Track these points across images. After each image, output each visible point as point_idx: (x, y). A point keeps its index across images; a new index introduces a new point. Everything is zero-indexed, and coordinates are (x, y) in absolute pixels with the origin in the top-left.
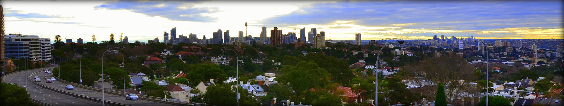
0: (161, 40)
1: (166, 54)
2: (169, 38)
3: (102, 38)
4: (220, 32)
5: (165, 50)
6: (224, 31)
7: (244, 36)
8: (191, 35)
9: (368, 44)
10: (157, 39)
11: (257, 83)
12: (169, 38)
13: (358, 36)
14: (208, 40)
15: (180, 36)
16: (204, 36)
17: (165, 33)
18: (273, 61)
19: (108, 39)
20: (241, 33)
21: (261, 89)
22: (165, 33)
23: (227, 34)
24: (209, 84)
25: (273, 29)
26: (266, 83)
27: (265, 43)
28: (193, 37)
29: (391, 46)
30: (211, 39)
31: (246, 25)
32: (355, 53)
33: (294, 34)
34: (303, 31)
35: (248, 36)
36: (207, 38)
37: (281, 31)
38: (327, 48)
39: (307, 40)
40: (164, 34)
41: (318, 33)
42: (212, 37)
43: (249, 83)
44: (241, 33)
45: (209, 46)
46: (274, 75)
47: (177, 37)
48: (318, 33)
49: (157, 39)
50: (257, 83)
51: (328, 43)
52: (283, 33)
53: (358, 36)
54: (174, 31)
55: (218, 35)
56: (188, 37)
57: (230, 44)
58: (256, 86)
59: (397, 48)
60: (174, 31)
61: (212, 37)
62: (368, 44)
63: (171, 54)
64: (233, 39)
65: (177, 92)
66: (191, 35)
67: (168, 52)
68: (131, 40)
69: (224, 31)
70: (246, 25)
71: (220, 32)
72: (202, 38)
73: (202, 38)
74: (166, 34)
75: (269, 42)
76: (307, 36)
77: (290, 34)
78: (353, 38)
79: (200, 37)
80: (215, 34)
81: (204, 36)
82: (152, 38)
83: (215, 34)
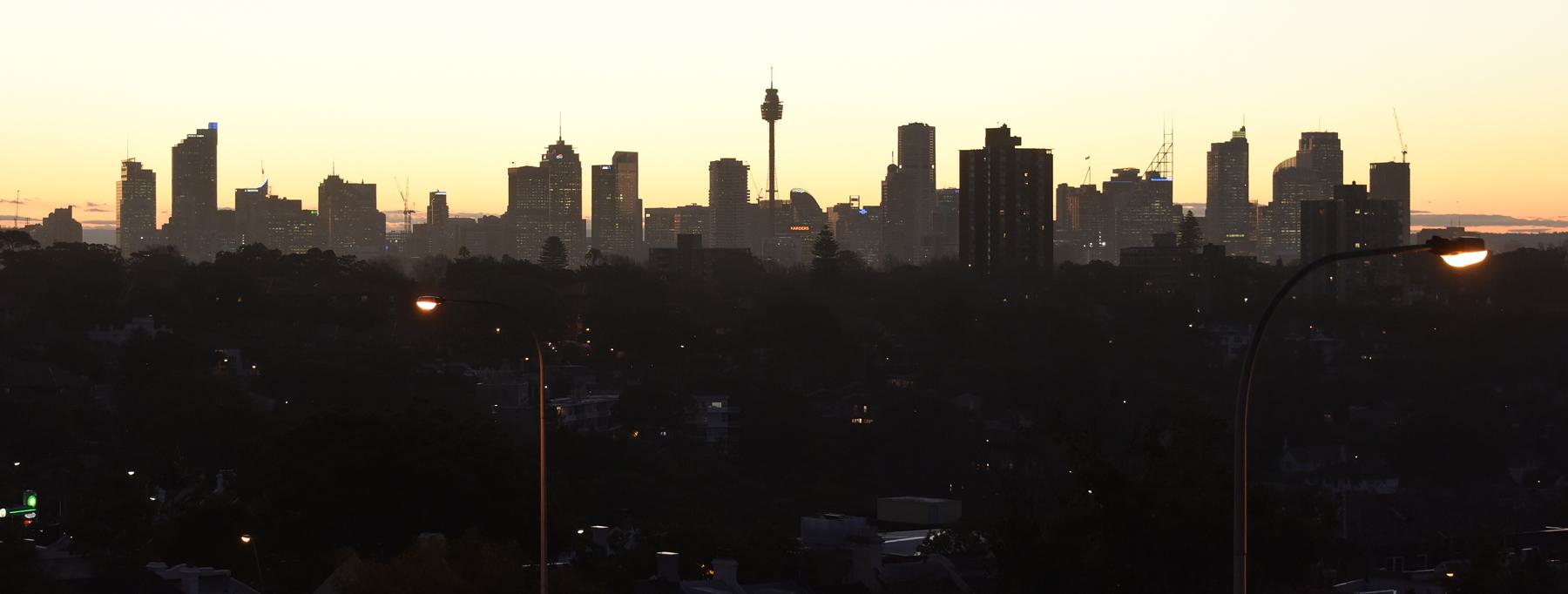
4: (562, 159)
6: (594, 154)
7: (757, 190)
8: (332, 188)
15: (241, 194)
16: (438, 201)
20: (728, 175)
25: (979, 143)
30: (488, 220)
31: (772, 109)
34: (1229, 160)
35: (783, 195)
36: (457, 206)
37: (1042, 161)
40: (117, 175)
41: (1356, 172)
44: (728, 175)
47: (226, 199)
48: (1356, 172)
52: (1066, 173)
54: (197, 156)
56: (311, 202)
66: (332, 188)
69: (594, 154)
70: (772, 109)
71: (562, 159)
74: (137, 180)
77: (1125, 178)
80: (520, 178)
81: (438, 201)
83: (520, 178)
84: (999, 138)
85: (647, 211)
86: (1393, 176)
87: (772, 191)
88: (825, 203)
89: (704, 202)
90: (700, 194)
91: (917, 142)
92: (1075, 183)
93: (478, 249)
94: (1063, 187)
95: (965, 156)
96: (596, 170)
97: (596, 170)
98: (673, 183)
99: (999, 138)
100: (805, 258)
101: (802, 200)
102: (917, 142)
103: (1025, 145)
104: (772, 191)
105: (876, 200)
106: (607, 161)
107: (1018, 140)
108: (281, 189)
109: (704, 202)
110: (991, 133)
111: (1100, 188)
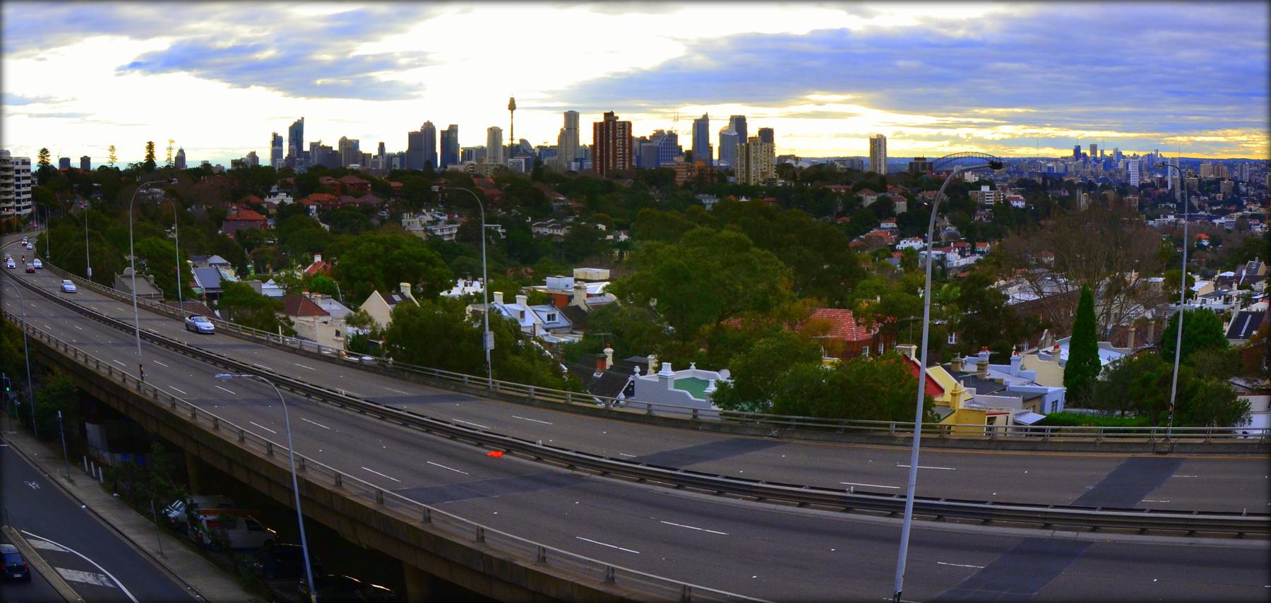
0: (265, 159)
1: (276, 201)
2: (285, 153)
3: (129, 156)
4: (429, 129)
5: (274, 189)
6: (441, 126)
7: (506, 142)
8: (344, 142)
9: (906, 169)
10: (253, 156)
11: (548, 299)
12: (285, 153)
13: (878, 144)
14: (391, 157)
15: (313, 145)
16: (382, 146)
17: (275, 135)
18: (602, 227)
19: (141, 158)
20: (495, 134)
21: (561, 320)
22: (275, 135)
23: (450, 136)
24: (397, 298)
26: (580, 301)
27: (574, 166)
28: (349, 147)
29: (970, 177)
30: (401, 155)
31: (512, 106)
32: (869, 199)
33: (673, 137)
34: (701, 127)
35: (517, 142)
36: (389, 150)
37: (627, 126)
38: (780, 183)
39: (716, 156)
40: (271, 138)
41: (752, 131)
43: (522, 299)
44: (495, 134)
45: (395, 175)
46: (605, 273)
47: (306, 148)
48: (752, 131)
49: (253, 156)
50: (548, 299)
51: (786, 166)
52: (636, 133)
53: (878, 144)
54: (297, 131)
55: (422, 139)
56: (336, 148)
57: (461, 168)
58: (545, 311)
59: (985, 183)
60: (297, 131)
62: (906, 169)
63: (289, 200)
64: (468, 153)
65: (310, 319)
66: (344, 142)
67: (282, 196)
68: (193, 161)
69: (441, 126)
70: (512, 106)
71: (429, 129)
72: (375, 152)
73: (375, 152)
74: (277, 141)
75: (588, 164)
76: (714, 141)
77: (659, 135)
78: (864, 151)
79: (368, 147)
81: (382, 146)
82: (242, 154)
83: (413, 137)
86: (767, 135)
88: (534, 144)
89: (485, 144)
90: (481, 141)
93: (397, 164)
96: (442, 132)
97: (442, 132)
105: (556, 144)
106: (446, 128)
108: (326, 143)
109: (485, 144)
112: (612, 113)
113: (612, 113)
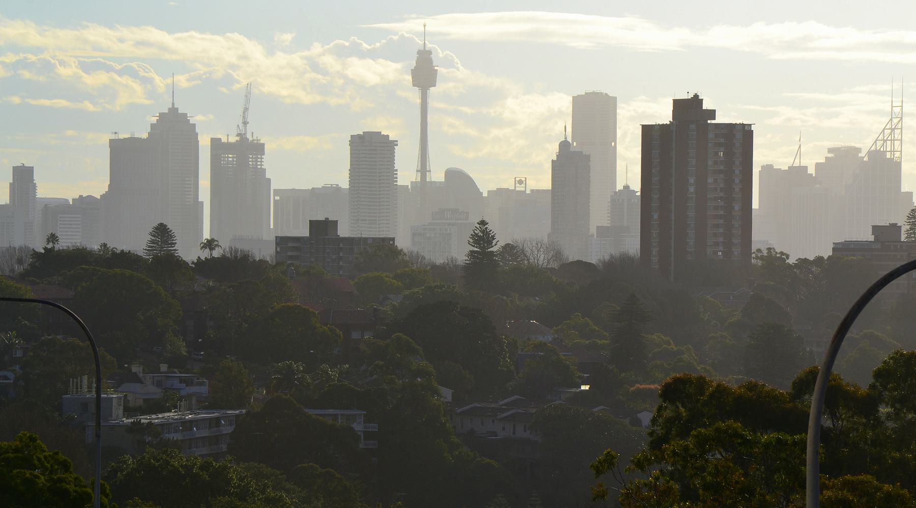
4: (174, 128)
6: (211, 128)
7: (406, 174)
20: (371, 152)
31: (424, 73)
35: (437, 175)
37: (740, 138)
42: (97, 184)
44: (371, 152)
61: (97, 184)
69: (211, 128)
70: (424, 73)
71: (174, 128)
77: (842, 157)
80: (122, 152)
83: (122, 152)
84: (689, 110)
85: (277, 192)
87: (423, 169)
88: (486, 184)
89: (344, 182)
91: (594, 112)
92: (783, 162)
94: (768, 169)
95: (648, 131)
97: (216, 143)
98: (306, 166)
99: (689, 110)
100: (459, 252)
101: (458, 179)
102: (594, 112)
103: (720, 119)
104: (423, 169)
107: (712, 114)
110: (679, 105)
111: (812, 171)
112: (696, 101)
113: (696, 101)
